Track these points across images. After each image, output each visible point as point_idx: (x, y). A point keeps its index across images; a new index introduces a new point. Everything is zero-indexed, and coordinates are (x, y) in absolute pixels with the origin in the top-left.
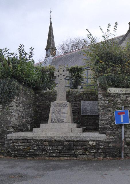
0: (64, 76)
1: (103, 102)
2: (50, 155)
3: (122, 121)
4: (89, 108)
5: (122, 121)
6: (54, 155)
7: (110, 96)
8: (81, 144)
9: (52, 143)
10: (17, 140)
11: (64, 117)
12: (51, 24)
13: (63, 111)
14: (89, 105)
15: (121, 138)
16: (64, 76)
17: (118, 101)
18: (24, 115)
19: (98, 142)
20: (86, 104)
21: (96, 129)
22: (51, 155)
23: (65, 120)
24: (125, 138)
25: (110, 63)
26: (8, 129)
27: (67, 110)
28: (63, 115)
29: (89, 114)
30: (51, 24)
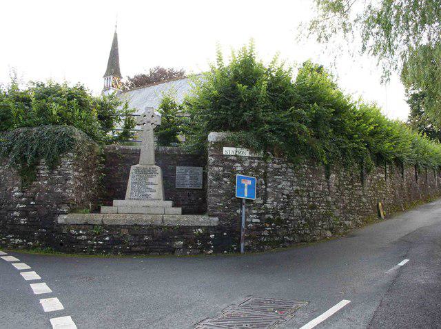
0: (152, 124)
1: (216, 169)
2: (130, 249)
3: (246, 195)
4: (189, 177)
5: (246, 195)
6: (138, 249)
7: (226, 160)
8: (183, 231)
9: (136, 229)
10: (77, 226)
11: (151, 190)
12: (116, 34)
13: (150, 180)
14: (188, 173)
15: (241, 223)
16: (152, 124)
17: (238, 169)
18: (84, 184)
19: (208, 229)
20: (184, 171)
21: (201, 211)
22: (133, 249)
23: (153, 195)
24: (247, 223)
25: (365, 125)
26: (60, 208)
27: (156, 180)
28: (150, 186)
29: (188, 187)
30: (116, 34)
